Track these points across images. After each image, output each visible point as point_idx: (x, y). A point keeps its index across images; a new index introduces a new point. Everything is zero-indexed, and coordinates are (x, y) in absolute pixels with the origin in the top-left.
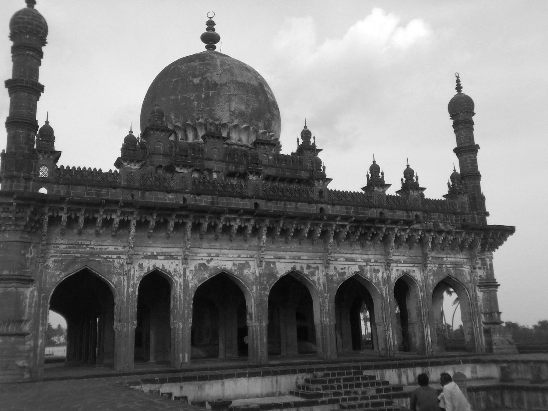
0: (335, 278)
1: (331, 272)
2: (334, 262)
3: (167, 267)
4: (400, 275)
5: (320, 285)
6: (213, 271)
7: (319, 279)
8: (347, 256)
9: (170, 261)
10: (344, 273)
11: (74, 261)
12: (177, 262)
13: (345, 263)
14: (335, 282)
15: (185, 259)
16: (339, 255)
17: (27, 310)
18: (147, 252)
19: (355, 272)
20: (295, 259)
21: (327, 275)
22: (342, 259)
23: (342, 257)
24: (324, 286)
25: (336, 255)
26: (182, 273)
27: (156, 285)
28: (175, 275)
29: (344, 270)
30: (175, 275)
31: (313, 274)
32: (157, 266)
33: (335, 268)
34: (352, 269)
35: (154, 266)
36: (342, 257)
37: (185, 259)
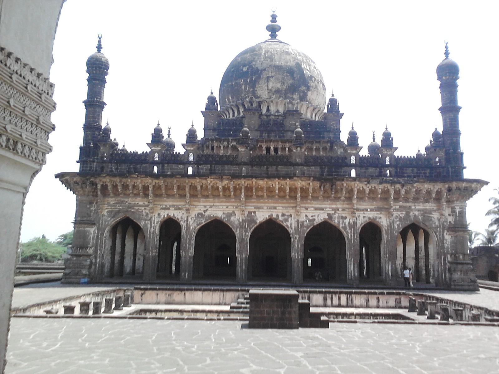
0: (305, 223)
1: (302, 218)
2: (305, 211)
3: (176, 215)
4: (366, 221)
5: (292, 229)
6: (207, 218)
7: (291, 224)
8: (317, 206)
9: (178, 211)
10: (314, 220)
11: (119, 212)
12: (183, 212)
13: (315, 211)
14: (305, 227)
15: (188, 210)
16: (310, 205)
17: (91, 241)
18: (162, 205)
19: (324, 219)
20: (271, 209)
21: (298, 221)
22: (313, 209)
23: (312, 207)
24: (295, 229)
25: (307, 205)
26: (186, 219)
27: (171, 228)
28: (181, 221)
29: (314, 217)
30: (181, 221)
31: (287, 220)
32: (170, 215)
33: (306, 216)
34: (320, 217)
35: (168, 215)
36: (312, 207)
37: (188, 210)
